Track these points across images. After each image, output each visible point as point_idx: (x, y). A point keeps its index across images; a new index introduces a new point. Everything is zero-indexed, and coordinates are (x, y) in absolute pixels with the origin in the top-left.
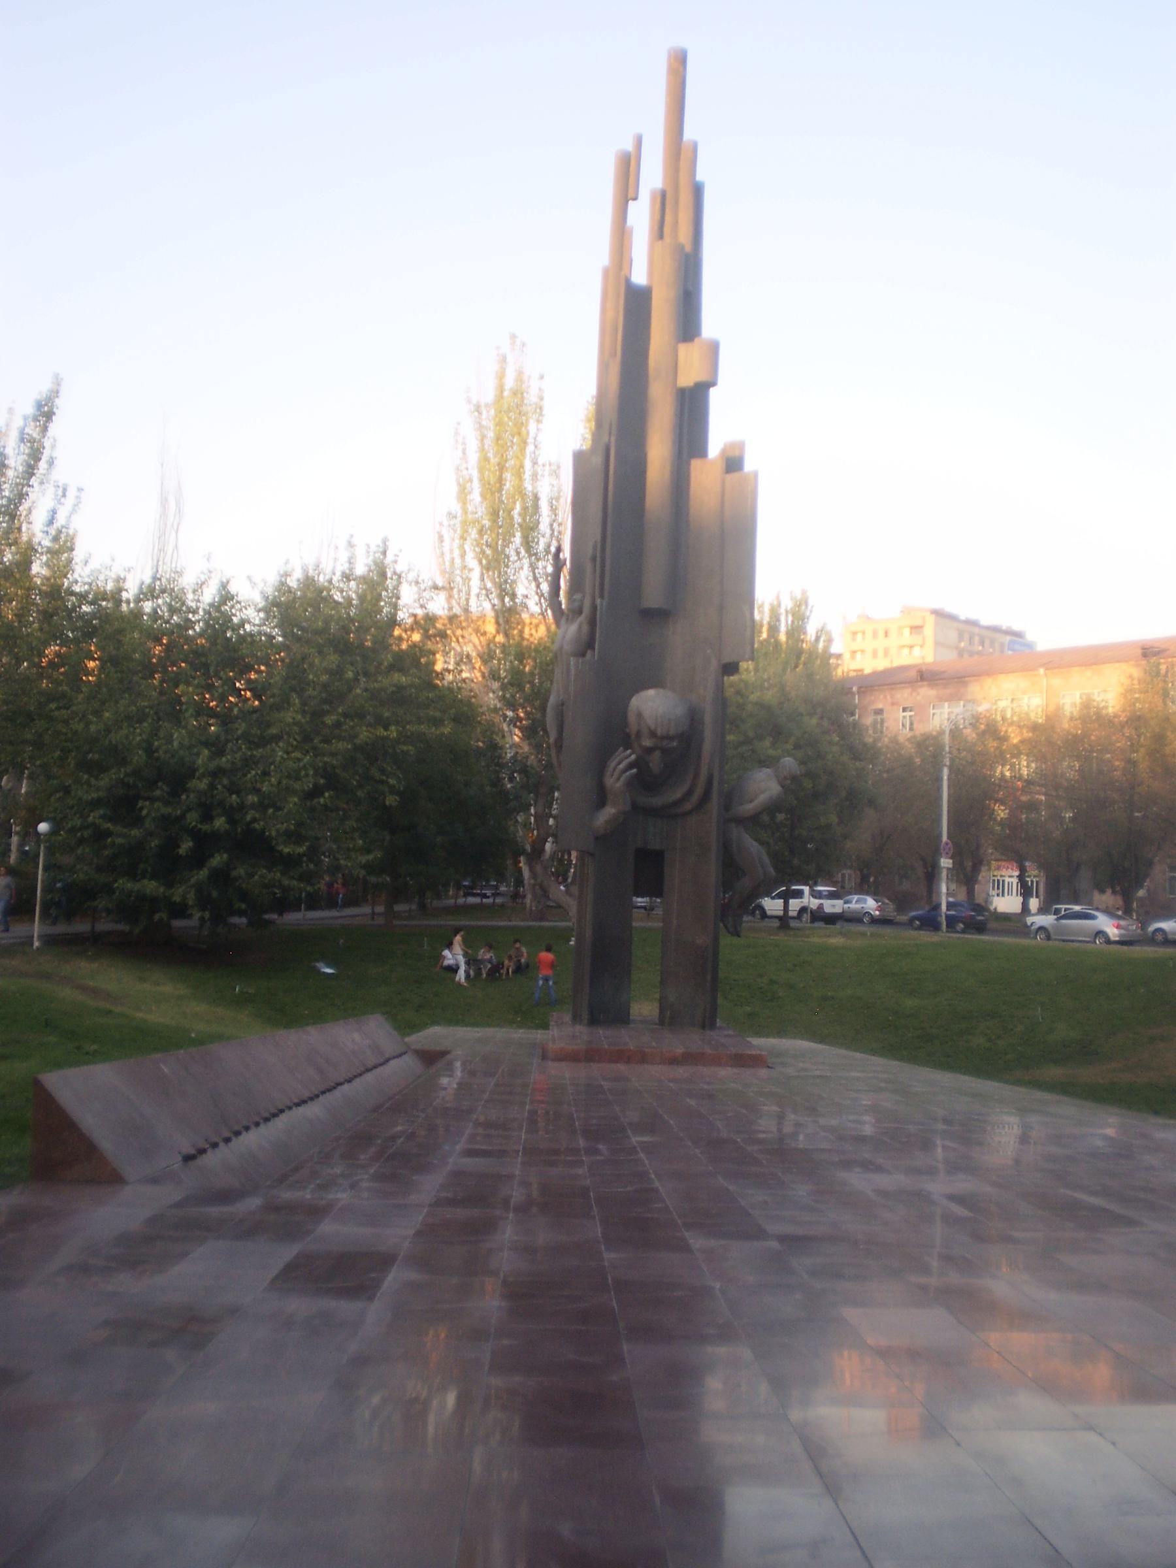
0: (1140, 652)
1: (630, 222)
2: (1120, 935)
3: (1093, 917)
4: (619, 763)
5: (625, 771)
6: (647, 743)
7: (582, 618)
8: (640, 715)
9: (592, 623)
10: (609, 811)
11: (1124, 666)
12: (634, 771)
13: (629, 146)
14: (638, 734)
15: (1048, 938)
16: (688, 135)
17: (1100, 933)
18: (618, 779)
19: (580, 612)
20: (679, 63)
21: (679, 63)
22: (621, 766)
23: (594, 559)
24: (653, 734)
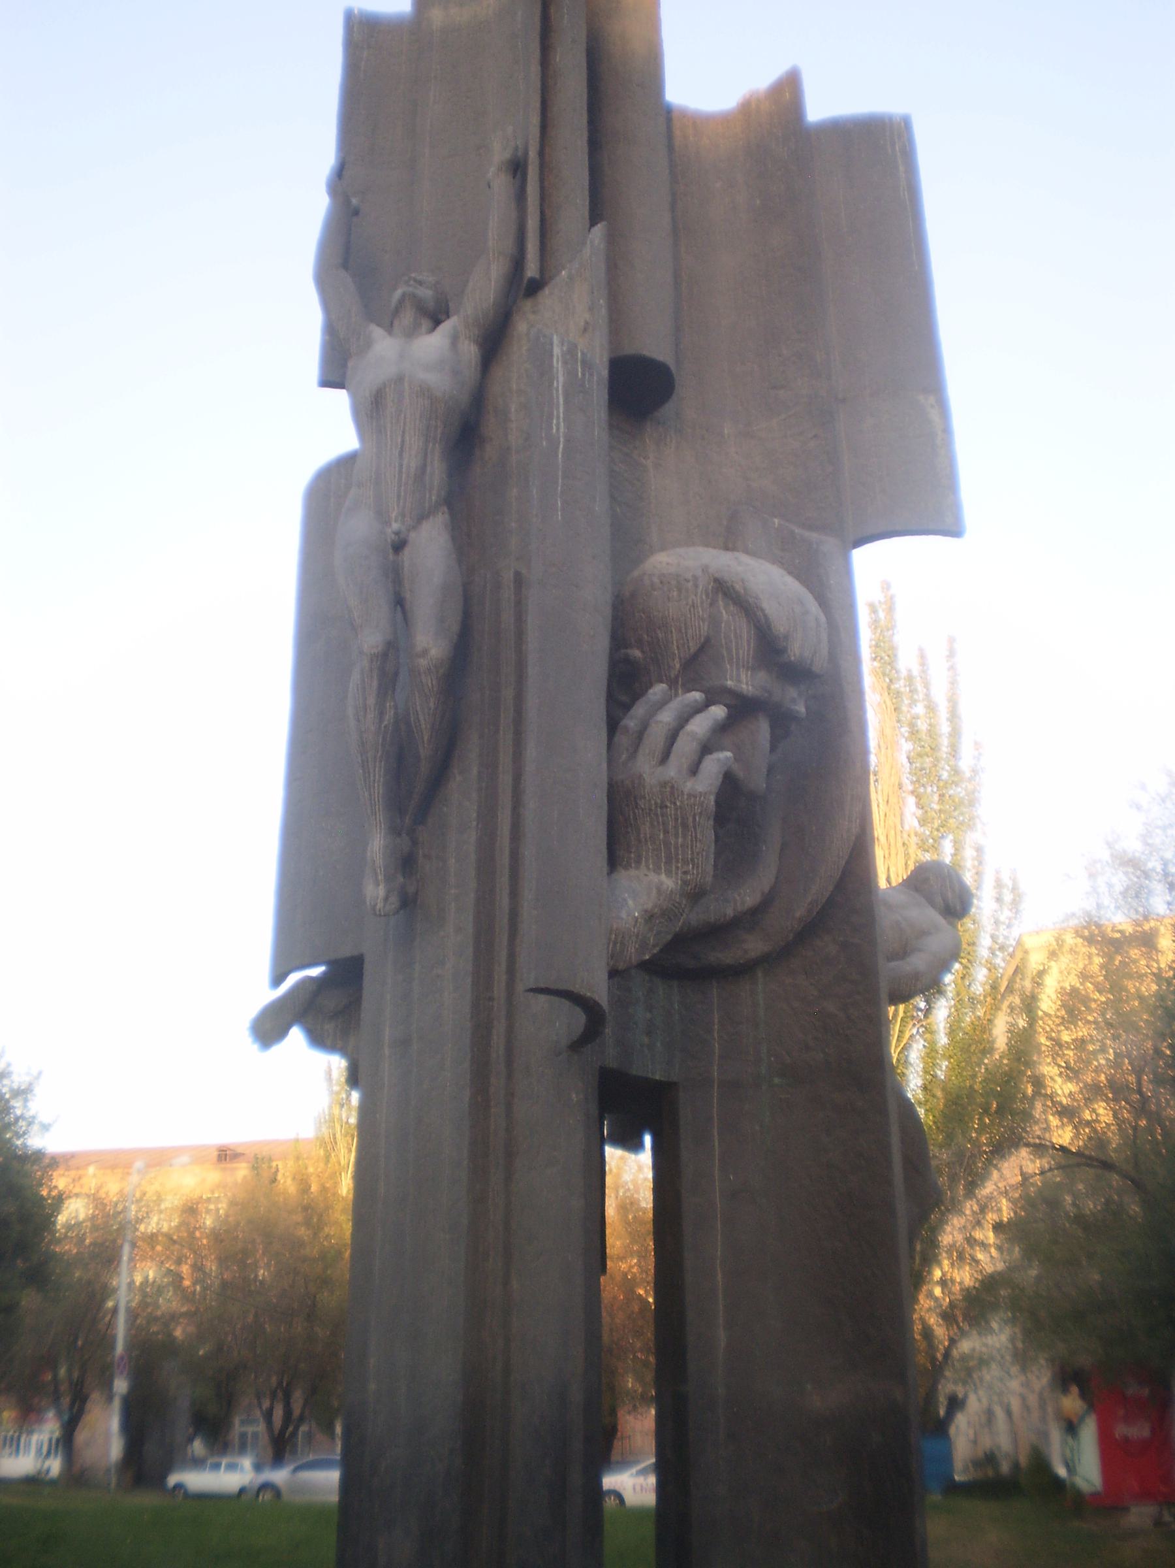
0: (216, 1153)
5: (706, 749)
9: (493, 340)
18: (694, 771)
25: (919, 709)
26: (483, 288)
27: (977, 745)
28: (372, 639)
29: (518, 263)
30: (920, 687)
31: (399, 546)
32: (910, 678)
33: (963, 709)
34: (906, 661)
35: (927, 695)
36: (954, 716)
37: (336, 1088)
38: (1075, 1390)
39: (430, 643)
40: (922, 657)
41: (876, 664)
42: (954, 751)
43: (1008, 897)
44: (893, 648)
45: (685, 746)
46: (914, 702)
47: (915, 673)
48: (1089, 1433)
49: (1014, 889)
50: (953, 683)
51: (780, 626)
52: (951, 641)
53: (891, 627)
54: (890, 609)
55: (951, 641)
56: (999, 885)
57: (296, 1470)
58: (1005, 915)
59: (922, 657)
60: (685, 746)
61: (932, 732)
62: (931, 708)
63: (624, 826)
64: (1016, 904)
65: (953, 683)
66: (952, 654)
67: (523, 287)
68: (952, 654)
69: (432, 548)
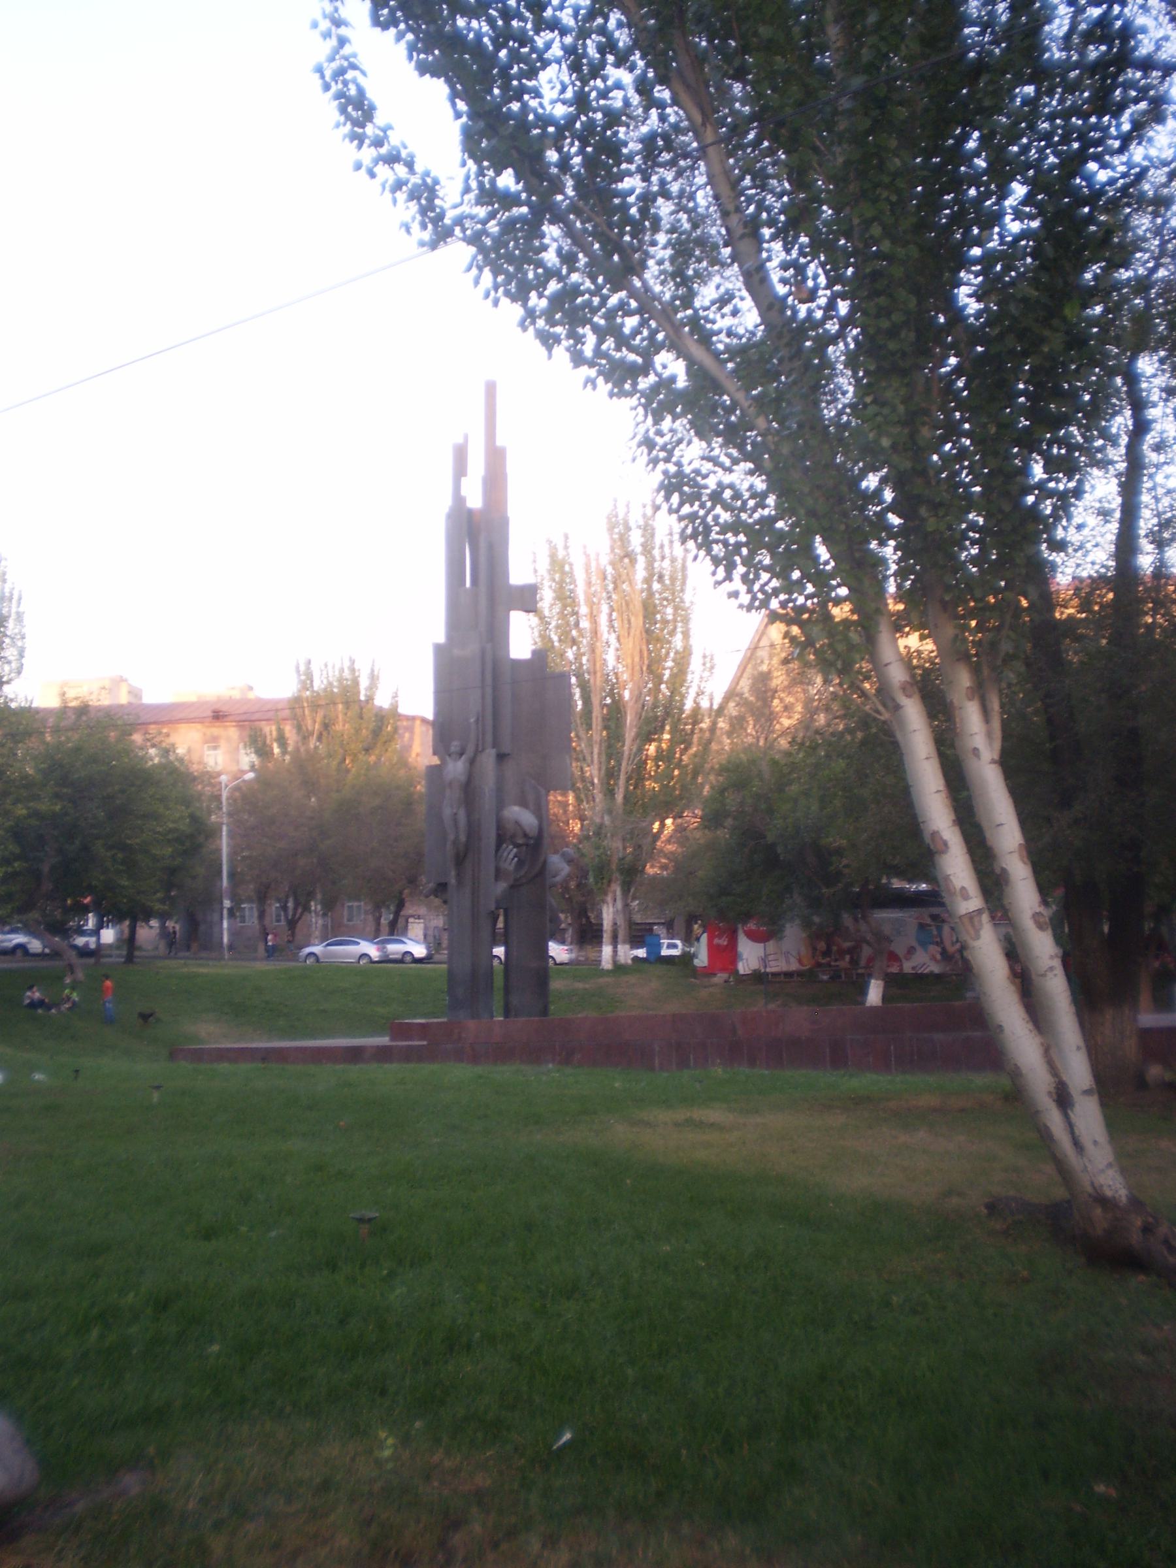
1: (463, 493)
3: (358, 943)
6: (520, 841)
7: (463, 757)
8: (517, 823)
9: (472, 762)
10: (502, 886)
11: (199, 726)
13: (461, 441)
14: (513, 836)
15: (318, 960)
16: (499, 443)
19: (461, 754)
20: (491, 390)
21: (491, 390)
22: (511, 856)
23: (477, 721)
24: (525, 835)
25: (666, 563)
26: (470, 752)
28: (451, 837)
29: (477, 745)
30: (667, 550)
32: (662, 547)
37: (303, 677)
39: (463, 838)
42: (682, 590)
43: (708, 665)
44: (653, 529)
45: (509, 861)
46: (663, 558)
49: (712, 659)
51: (528, 831)
56: (705, 657)
57: (328, 945)
58: (706, 674)
60: (509, 861)
63: (499, 874)
64: (712, 668)
67: (478, 751)
69: (462, 814)
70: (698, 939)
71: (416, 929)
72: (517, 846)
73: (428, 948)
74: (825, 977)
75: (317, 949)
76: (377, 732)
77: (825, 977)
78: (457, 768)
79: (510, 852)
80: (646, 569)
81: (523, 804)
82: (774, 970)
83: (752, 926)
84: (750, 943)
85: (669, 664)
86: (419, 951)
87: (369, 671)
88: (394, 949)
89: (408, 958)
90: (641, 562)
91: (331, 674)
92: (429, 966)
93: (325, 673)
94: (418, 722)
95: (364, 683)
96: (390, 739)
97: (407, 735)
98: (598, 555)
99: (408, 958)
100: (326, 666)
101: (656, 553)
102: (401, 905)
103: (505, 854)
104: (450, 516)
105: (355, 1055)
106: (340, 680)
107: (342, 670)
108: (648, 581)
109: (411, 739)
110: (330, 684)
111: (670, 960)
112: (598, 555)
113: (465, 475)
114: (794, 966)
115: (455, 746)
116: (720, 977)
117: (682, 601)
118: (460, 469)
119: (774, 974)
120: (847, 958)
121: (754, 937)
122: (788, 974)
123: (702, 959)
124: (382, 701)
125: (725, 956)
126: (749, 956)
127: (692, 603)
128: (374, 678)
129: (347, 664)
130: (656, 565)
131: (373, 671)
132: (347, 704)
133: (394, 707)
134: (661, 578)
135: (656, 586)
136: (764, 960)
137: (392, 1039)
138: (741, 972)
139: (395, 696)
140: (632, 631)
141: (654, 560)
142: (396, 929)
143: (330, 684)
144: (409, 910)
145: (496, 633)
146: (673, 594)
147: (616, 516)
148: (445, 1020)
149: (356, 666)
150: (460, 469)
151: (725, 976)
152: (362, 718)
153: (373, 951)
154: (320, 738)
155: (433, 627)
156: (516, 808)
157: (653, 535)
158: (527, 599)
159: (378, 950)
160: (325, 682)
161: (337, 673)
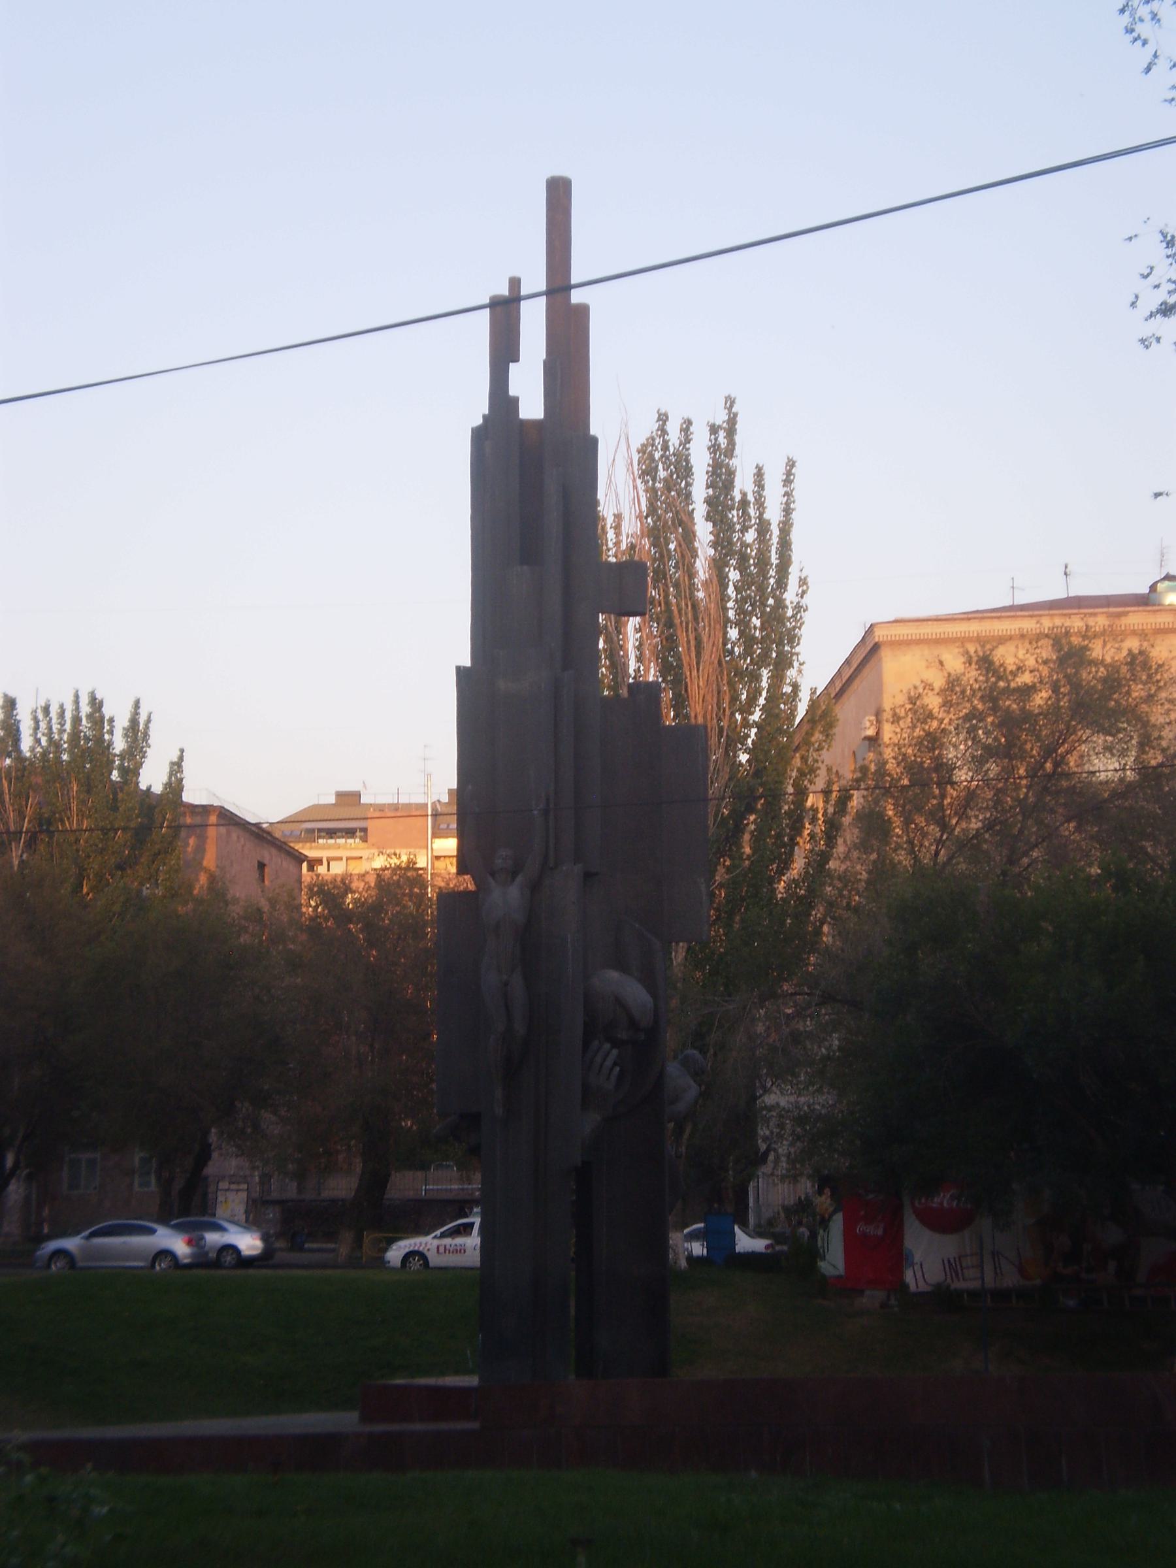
2: (193, 1255)
3: (152, 1232)
4: (604, 1060)
6: (623, 1035)
7: (519, 879)
8: (618, 1001)
9: (535, 887)
12: (618, 1069)
13: (504, 291)
17: (166, 1253)
18: (608, 1079)
19: (514, 874)
20: (559, 194)
21: (559, 194)
22: (609, 1062)
23: (546, 812)
24: (633, 1024)
25: (750, 536)
27: (803, 582)
30: (752, 511)
31: (506, 984)
32: (744, 503)
33: (795, 536)
34: (743, 483)
35: (760, 517)
36: (785, 545)
38: (827, 1191)
40: (759, 475)
41: (710, 491)
42: (782, 584)
44: (731, 473)
46: (745, 529)
47: (751, 498)
48: (837, 1224)
50: (788, 511)
52: (791, 464)
53: (730, 451)
54: (731, 432)
55: (791, 464)
59: (759, 475)
61: (763, 561)
62: (763, 528)
65: (788, 511)
66: (788, 481)
68: (788, 481)
70: (825, 1223)
71: (232, 1202)
72: (615, 1044)
73: (265, 1238)
74: (1071, 1303)
75: (71, 1244)
76: (142, 834)
77: (1071, 1303)
78: (507, 899)
79: (608, 1056)
80: (715, 545)
81: (623, 968)
82: (974, 1285)
83: (944, 1200)
84: (927, 1234)
85: (756, 716)
86: (248, 1243)
87: (126, 724)
88: (213, 1238)
89: (229, 1258)
90: (704, 531)
91: (55, 727)
92: (264, 1272)
93: (43, 725)
94: (213, 819)
95: (119, 744)
96: (168, 848)
97: (192, 841)
98: (618, 517)
99: (229, 1258)
100: (46, 710)
101: (734, 515)
102: (204, 1156)
103: (598, 1059)
104: (479, 435)
105: (318, 1452)
106: (75, 735)
107: (77, 720)
108: (718, 566)
109: (201, 849)
110: (55, 745)
111: (751, 1258)
112: (618, 517)
113: (516, 359)
114: (1011, 1279)
115: (503, 857)
116: (871, 1298)
117: (780, 604)
118: (505, 348)
119: (973, 1294)
120: (1112, 1266)
121: (939, 1222)
122: (1001, 1295)
123: (834, 1259)
124: (152, 778)
125: (880, 1257)
126: (928, 1258)
127: (798, 608)
128: (137, 735)
129: (85, 709)
130: (736, 537)
131: (134, 722)
132: (88, 787)
133: (175, 787)
134: (743, 558)
135: (734, 575)
136: (953, 1267)
137: (365, 1418)
138: (913, 1288)
139: (177, 766)
140: (705, 656)
141: (731, 527)
142: (189, 1205)
143: (55, 745)
144: (210, 1170)
145: (574, 649)
146: (761, 589)
147: (665, 447)
148: (473, 1381)
149: (107, 712)
150: (505, 348)
151: (880, 1294)
152: (115, 809)
153: (180, 1246)
154: (31, 844)
155: (448, 637)
156: (614, 975)
157: (729, 485)
158: (627, 588)
159: (190, 1242)
160: (44, 742)
161: (68, 726)
